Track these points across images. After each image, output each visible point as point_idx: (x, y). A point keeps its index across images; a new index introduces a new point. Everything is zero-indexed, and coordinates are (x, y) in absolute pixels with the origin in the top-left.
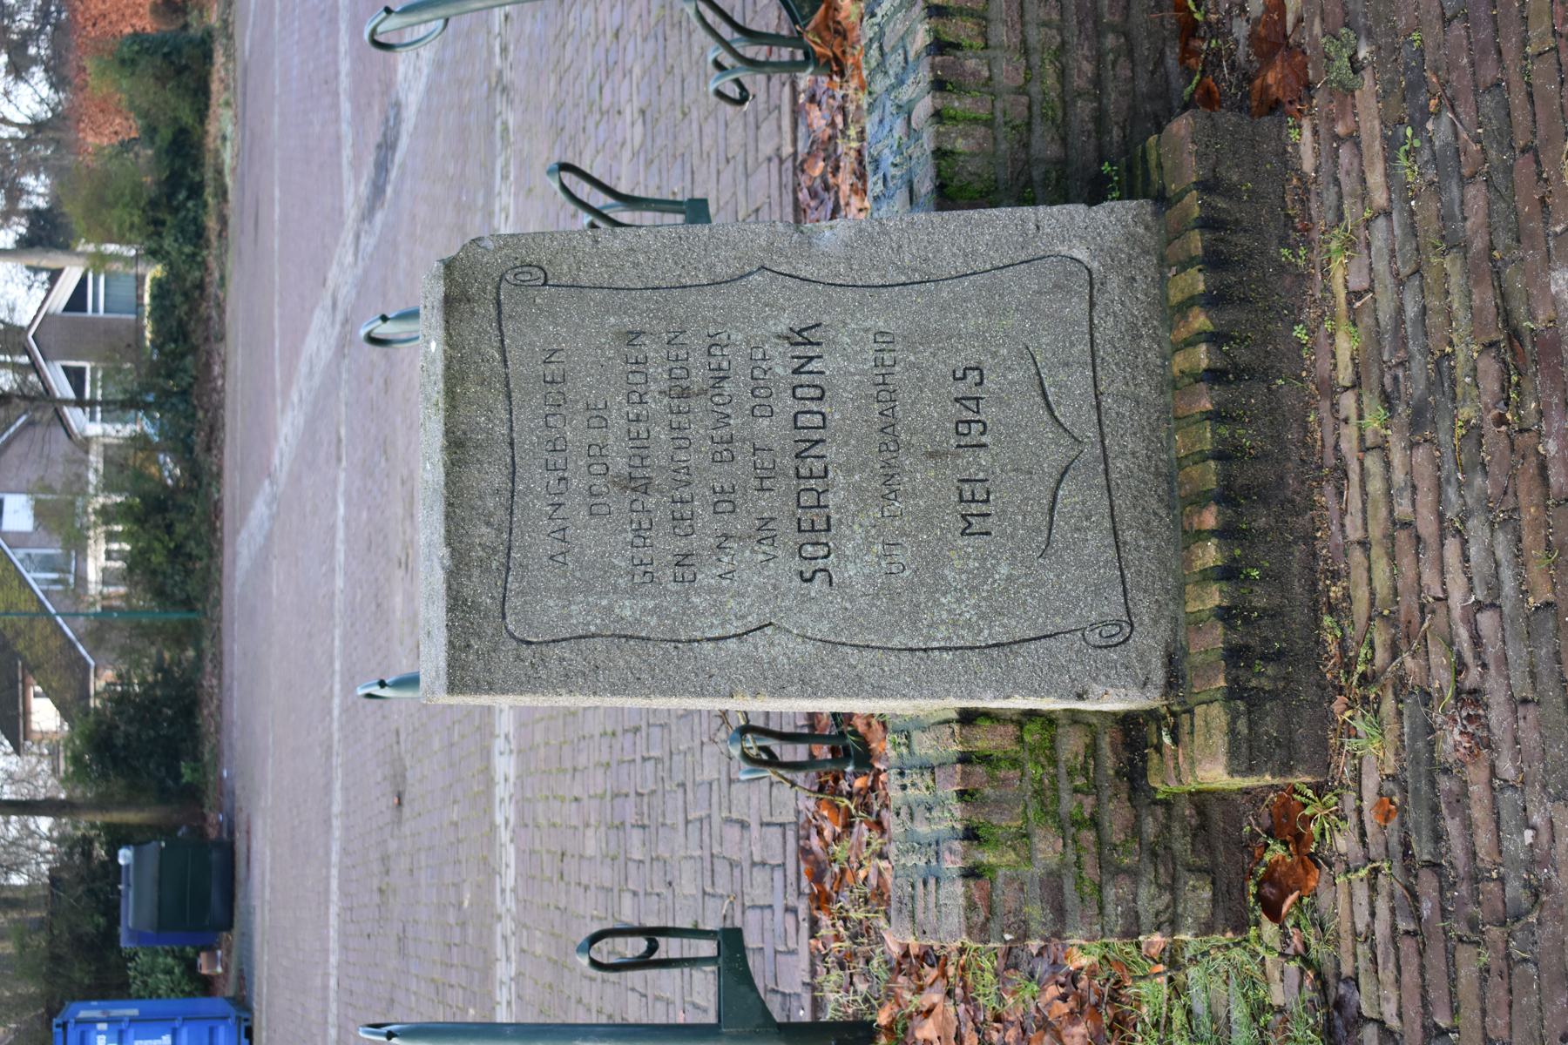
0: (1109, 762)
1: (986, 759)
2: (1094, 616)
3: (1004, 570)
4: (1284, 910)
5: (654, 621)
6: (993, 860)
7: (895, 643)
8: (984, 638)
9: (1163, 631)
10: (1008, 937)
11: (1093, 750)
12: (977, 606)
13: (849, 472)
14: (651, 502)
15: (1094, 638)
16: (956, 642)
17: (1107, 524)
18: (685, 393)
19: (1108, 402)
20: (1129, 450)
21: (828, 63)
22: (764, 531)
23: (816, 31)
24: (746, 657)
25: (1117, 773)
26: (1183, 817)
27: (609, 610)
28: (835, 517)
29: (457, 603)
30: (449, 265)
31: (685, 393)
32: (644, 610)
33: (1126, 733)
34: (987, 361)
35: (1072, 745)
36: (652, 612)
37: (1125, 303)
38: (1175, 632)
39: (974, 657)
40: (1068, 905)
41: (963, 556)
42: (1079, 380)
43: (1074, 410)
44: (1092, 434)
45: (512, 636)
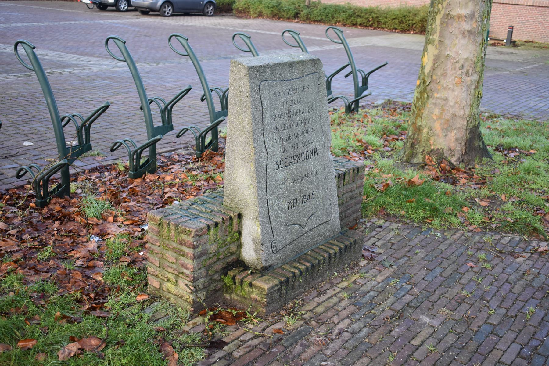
0: (229, 260)
1: (231, 224)
2: (277, 242)
3: (283, 215)
4: (218, 320)
5: (266, 123)
6: (211, 233)
7: (268, 190)
8: (271, 214)
9: (276, 262)
10: (195, 243)
11: (232, 254)
12: (276, 210)
13: (296, 170)
14: (287, 118)
15: (273, 244)
16: (269, 206)
17: (293, 240)
18: (305, 124)
19: (311, 232)
20: (304, 240)
21: (201, 157)
22: (284, 149)
23: (210, 152)
24: (262, 151)
25: (227, 263)
26: (217, 285)
27: (267, 110)
28: (288, 167)
29: (265, 67)
30: (319, 60)
31: (305, 124)
32: (268, 120)
33: (235, 262)
34: (315, 199)
35: (233, 248)
36: (268, 122)
37: (325, 228)
38: (276, 265)
39: (267, 213)
40: (201, 259)
41: (284, 203)
42: (314, 224)
43: (312, 223)
44: (307, 230)
45: (260, 84)
